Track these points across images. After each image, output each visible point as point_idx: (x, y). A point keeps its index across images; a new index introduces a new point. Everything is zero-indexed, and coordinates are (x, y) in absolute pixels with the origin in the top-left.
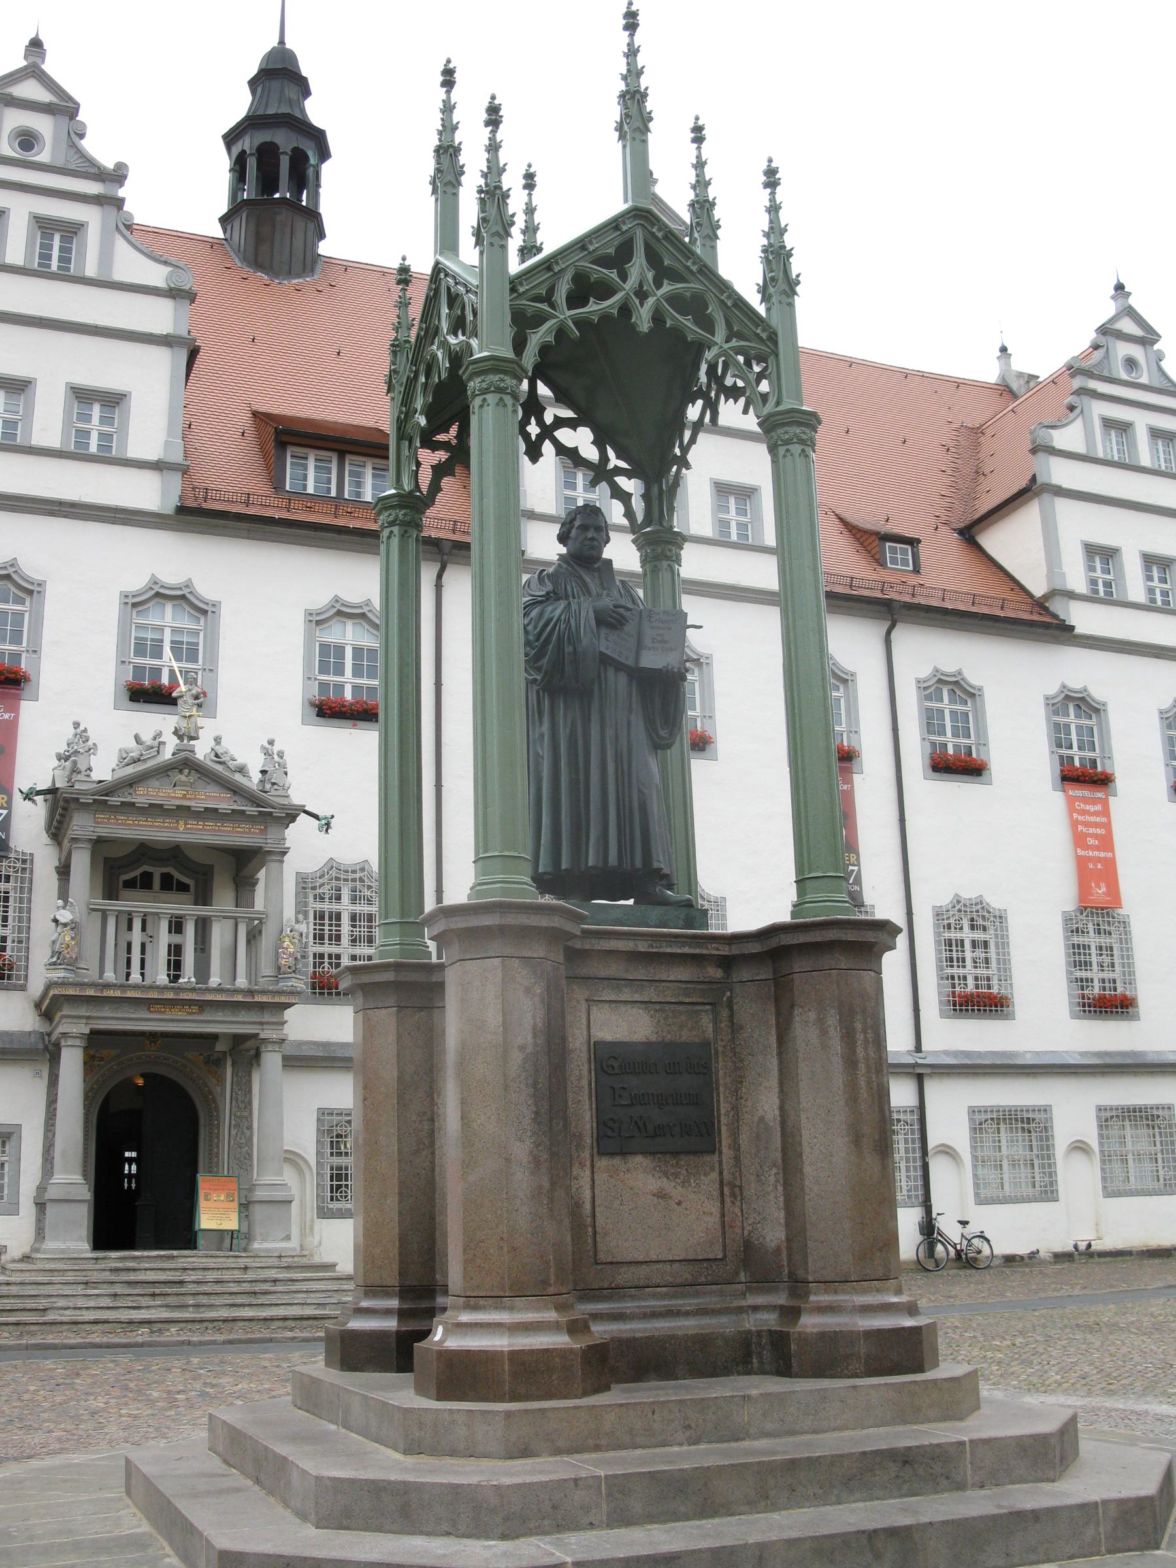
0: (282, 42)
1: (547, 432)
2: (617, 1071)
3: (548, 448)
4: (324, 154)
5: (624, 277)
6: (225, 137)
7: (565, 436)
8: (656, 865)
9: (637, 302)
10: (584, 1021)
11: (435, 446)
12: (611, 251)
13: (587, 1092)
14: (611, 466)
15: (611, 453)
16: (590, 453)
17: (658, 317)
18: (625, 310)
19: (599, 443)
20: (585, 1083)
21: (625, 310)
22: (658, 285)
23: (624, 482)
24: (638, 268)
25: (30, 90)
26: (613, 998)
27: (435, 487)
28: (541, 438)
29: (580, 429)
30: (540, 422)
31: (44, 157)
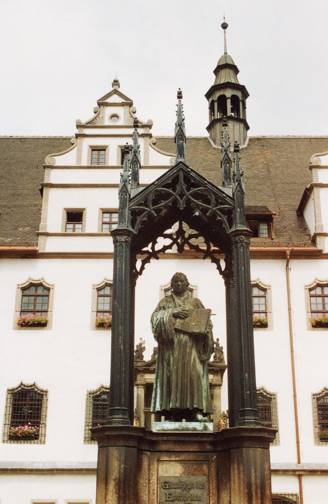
0: (226, 53)
1: (186, 241)
2: (167, 487)
4: (246, 95)
6: (206, 96)
7: (193, 241)
8: (195, 406)
10: (156, 468)
13: (156, 496)
15: (211, 245)
16: (204, 247)
19: (207, 242)
20: (156, 492)
21: (175, 202)
22: (188, 189)
24: (182, 185)
25: (115, 99)
26: (168, 459)
27: (142, 268)
30: (183, 237)
31: (121, 122)
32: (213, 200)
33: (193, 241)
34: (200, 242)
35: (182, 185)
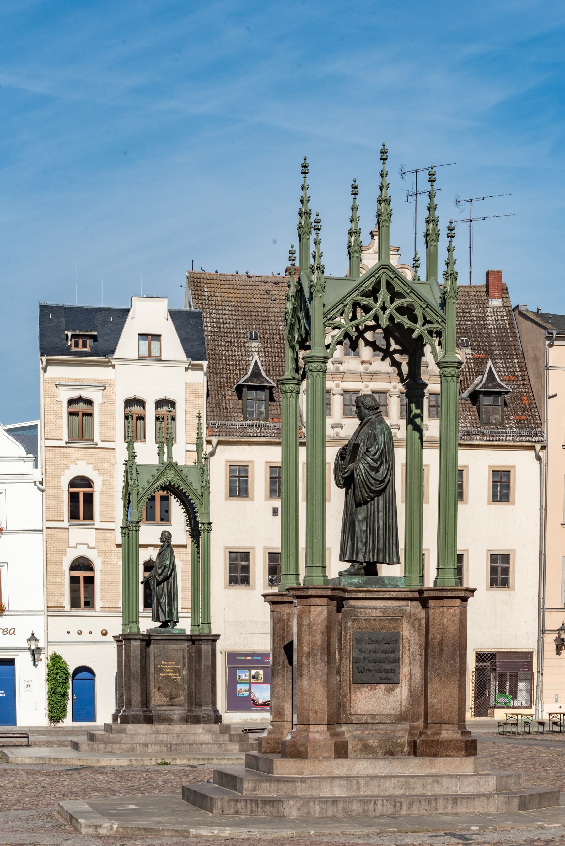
1: (361, 334)
3: (361, 343)
5: (376, 300)
7: (369, 335)
9: (381, 312)
12: (370, 288)
14: (391, 349)
15: (392, 342)
16: (382, 343)
17: (391, 318)
19: (387, 338)
22: (392, 301)
23: (397, 356)
24: (383, 295)
28: (357, 338)
32: (421, 320)
35: (383, 295)
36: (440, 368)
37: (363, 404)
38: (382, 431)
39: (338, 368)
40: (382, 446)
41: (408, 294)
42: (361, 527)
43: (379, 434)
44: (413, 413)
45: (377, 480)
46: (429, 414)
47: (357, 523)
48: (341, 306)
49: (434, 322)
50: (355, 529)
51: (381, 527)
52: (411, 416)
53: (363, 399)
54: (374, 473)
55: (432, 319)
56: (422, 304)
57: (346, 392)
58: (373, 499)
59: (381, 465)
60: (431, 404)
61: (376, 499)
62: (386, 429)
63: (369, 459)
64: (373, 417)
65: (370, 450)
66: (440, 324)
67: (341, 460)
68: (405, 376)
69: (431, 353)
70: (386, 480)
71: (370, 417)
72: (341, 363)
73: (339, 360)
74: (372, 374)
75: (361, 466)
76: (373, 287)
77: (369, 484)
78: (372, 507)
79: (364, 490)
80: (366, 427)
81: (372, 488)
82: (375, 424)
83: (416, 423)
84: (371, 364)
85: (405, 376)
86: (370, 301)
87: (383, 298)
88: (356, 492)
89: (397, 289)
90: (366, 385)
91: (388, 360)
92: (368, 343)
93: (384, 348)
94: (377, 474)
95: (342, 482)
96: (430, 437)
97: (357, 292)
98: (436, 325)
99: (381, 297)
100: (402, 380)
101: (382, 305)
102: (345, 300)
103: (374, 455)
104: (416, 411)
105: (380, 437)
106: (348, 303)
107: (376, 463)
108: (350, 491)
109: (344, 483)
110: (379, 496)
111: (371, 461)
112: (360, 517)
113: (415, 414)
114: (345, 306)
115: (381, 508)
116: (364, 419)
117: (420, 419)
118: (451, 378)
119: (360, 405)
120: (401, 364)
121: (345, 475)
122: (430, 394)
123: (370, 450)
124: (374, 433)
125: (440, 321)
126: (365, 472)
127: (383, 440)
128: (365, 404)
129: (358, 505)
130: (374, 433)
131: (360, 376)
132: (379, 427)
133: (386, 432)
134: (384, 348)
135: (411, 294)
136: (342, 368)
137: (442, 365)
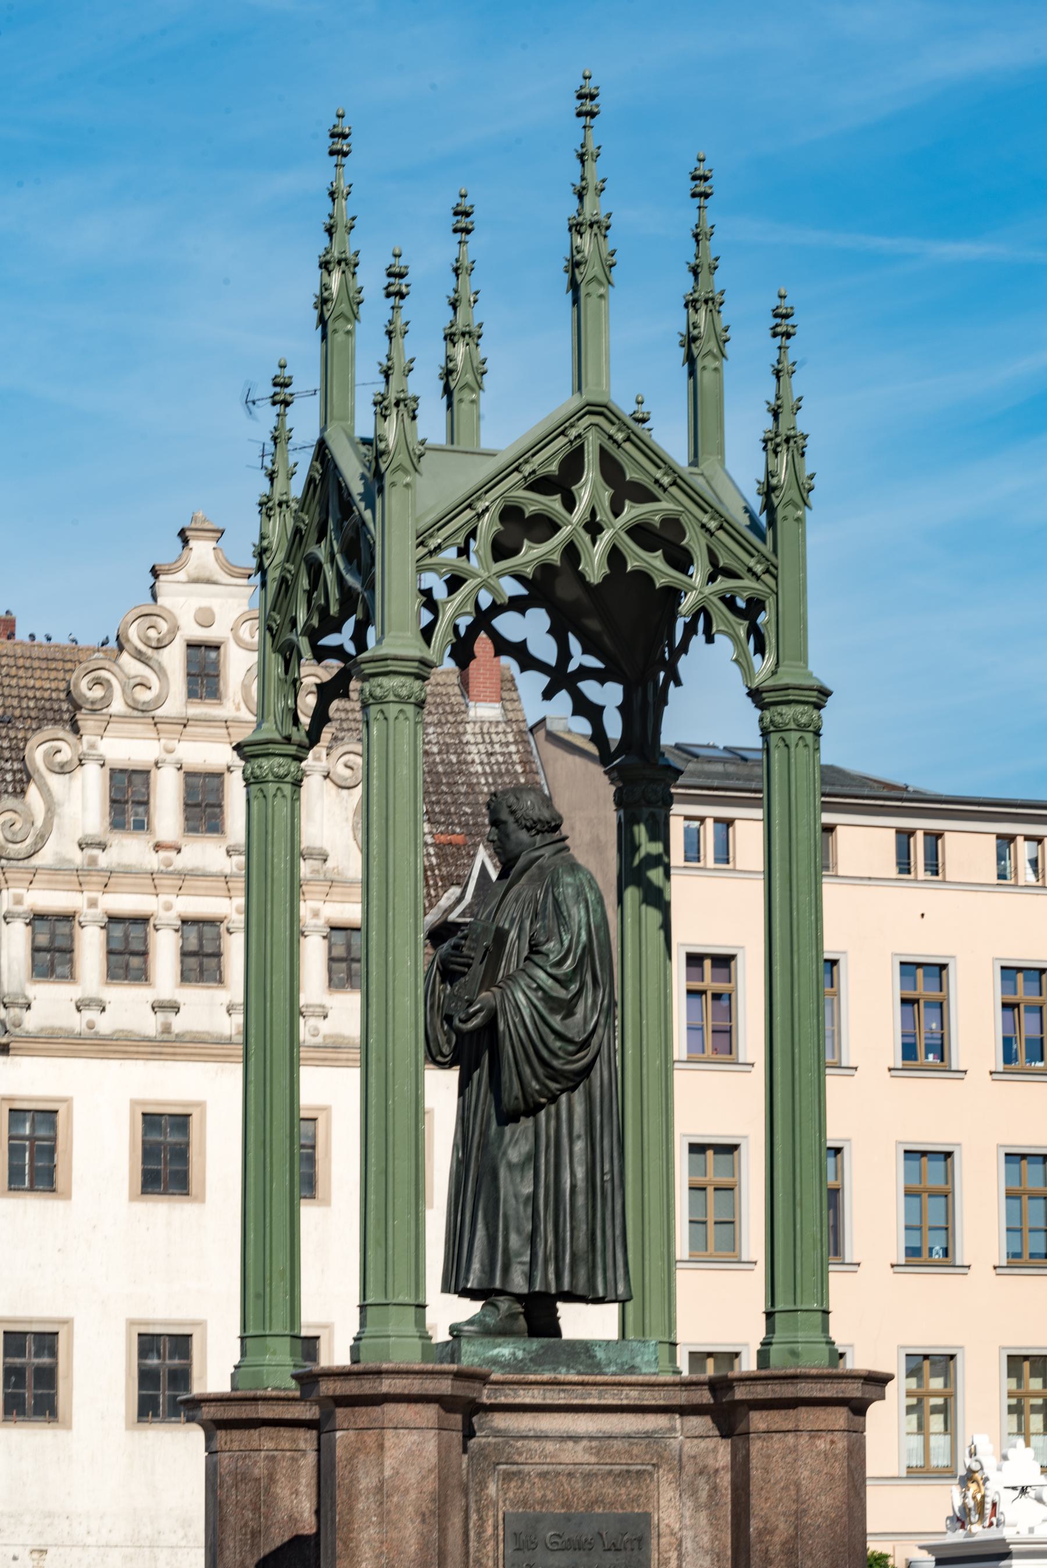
3: (483, 644)
5: (570, 504)
7: (509, 625)
9: (587, 538)
11: (320, 654)
12: (554, 468)
14: (572, 666)
15: (575, 645)
16: (545, 650)
17: (615, 556)
18: (571, 552)
19: (558, 632)
21: (571, 552)
23: (590, 688)
24: (590, 489)
27: (321, 717)
29: (530, 612)
33: (509, 625)
34: (532, 628)
36: (762, 706)
37: (513, 813)
38: (580, 893)
39: (93, 861)
40: (584, 937)
41: (665, 490)
42: (516, 1187)
43: (570, 903)
44: (643, 852)
45: (570, 1041)
46: (330, 980)
47: (503, 1172)
48: (469, 514)
49: (741, 570)
50: (497, 1189)
51: (581, 1183)
52: (636, 862)
53: (512, 800)
54: (559, 1018)
55: (735, 566)
56: (705, 519)
57: (114, 919)
58: (554, 1099)
59: (579, 993)
60: (335, 953)
61: (564, 1098)
62: (591, 888)
63: (541, 974)
64: (547, 852)
65: (544, 948)
66: (758, 578)
67: (443, 982)
68: (613, 747)
69: (736, 661)
70: (595, 1041)
71: (537, 853)
72: (103, 846)
73: (97, 840)
74: (183, 875)
75: (520, 997)
76: (562, 465)
77: (545, 1053)
78: (553, 1123)
79: (527, 1071)
80: (523, 880)
81: (556, 1063)
82: (555, 871)
83: (649, 882)
84: (179, 851)
85: (613, 747)
86: (554, 504)
87: (592, 497)
88: (505, 1077)
89: (631, 475)
90: (166, 903)
91: (563, 699)
92: (502, 646)
93: (553, 662)
94: (569, 1021)
95: (446, 1050)
96: (331, 1036)
97: (516, 477)
98: (748, 582)
99: (584, 495)
100: (605, 757)
101: (587, 515)
102: (479, 499)
103: (560, 963)
104: (649, 847)
105: (574, 911)
106: (487, 509)
107: (566, 988)
108: (476, 1075)
109: (454, 1050)
110: (573, 1089)
111: (550, 982)
112: (514, 1155)
113: (648, 856)
114: (480, 516)
115: (579, 1126)
116: (517, 858)
117: (660, 870)
118: (799, 734)
119: (505, 815)
120: (601, 709)
121: (471, 1025)
122: (333, 928)
123: (544, 948)
124: (555, 900)
125: (759, 569)
126: (532, 1016)
127: (584, 920)
128: (519, 814)
129: (508, 1117)
130: (555, 900)
131: (153, 881)
132: (569, 879)
133: (591, 897)
134: (553, 662)
135: (674, 490)
136: (104, 860)
137: (768, 698)
